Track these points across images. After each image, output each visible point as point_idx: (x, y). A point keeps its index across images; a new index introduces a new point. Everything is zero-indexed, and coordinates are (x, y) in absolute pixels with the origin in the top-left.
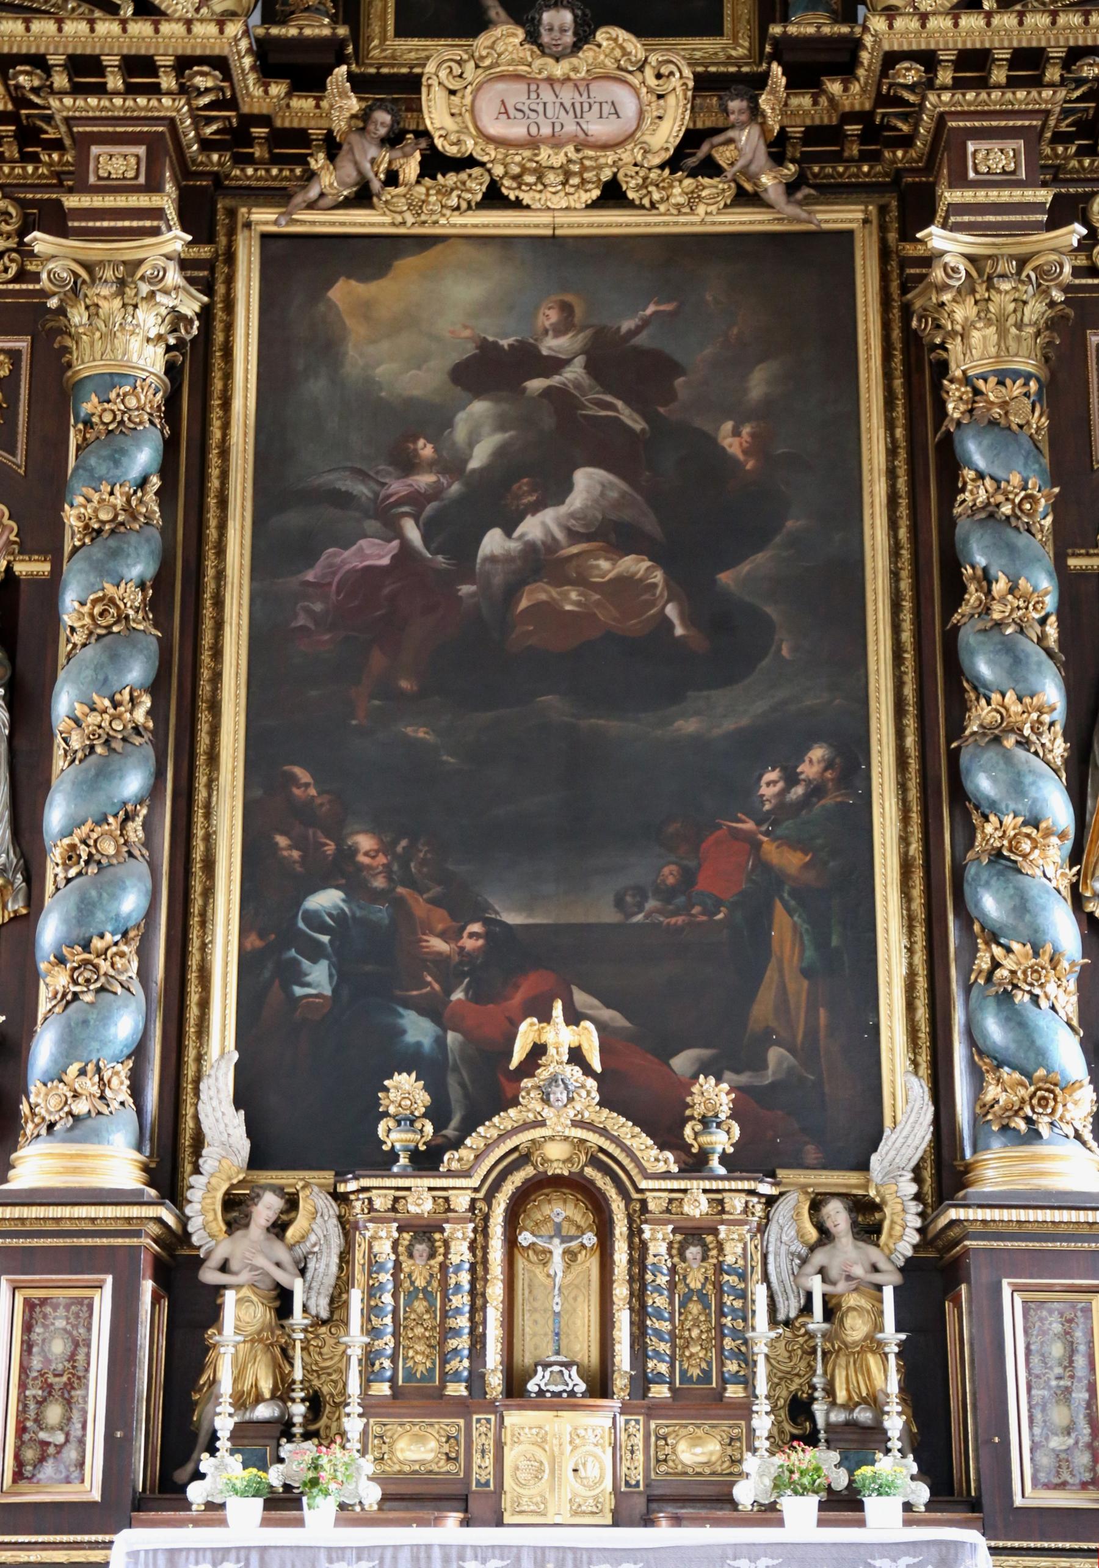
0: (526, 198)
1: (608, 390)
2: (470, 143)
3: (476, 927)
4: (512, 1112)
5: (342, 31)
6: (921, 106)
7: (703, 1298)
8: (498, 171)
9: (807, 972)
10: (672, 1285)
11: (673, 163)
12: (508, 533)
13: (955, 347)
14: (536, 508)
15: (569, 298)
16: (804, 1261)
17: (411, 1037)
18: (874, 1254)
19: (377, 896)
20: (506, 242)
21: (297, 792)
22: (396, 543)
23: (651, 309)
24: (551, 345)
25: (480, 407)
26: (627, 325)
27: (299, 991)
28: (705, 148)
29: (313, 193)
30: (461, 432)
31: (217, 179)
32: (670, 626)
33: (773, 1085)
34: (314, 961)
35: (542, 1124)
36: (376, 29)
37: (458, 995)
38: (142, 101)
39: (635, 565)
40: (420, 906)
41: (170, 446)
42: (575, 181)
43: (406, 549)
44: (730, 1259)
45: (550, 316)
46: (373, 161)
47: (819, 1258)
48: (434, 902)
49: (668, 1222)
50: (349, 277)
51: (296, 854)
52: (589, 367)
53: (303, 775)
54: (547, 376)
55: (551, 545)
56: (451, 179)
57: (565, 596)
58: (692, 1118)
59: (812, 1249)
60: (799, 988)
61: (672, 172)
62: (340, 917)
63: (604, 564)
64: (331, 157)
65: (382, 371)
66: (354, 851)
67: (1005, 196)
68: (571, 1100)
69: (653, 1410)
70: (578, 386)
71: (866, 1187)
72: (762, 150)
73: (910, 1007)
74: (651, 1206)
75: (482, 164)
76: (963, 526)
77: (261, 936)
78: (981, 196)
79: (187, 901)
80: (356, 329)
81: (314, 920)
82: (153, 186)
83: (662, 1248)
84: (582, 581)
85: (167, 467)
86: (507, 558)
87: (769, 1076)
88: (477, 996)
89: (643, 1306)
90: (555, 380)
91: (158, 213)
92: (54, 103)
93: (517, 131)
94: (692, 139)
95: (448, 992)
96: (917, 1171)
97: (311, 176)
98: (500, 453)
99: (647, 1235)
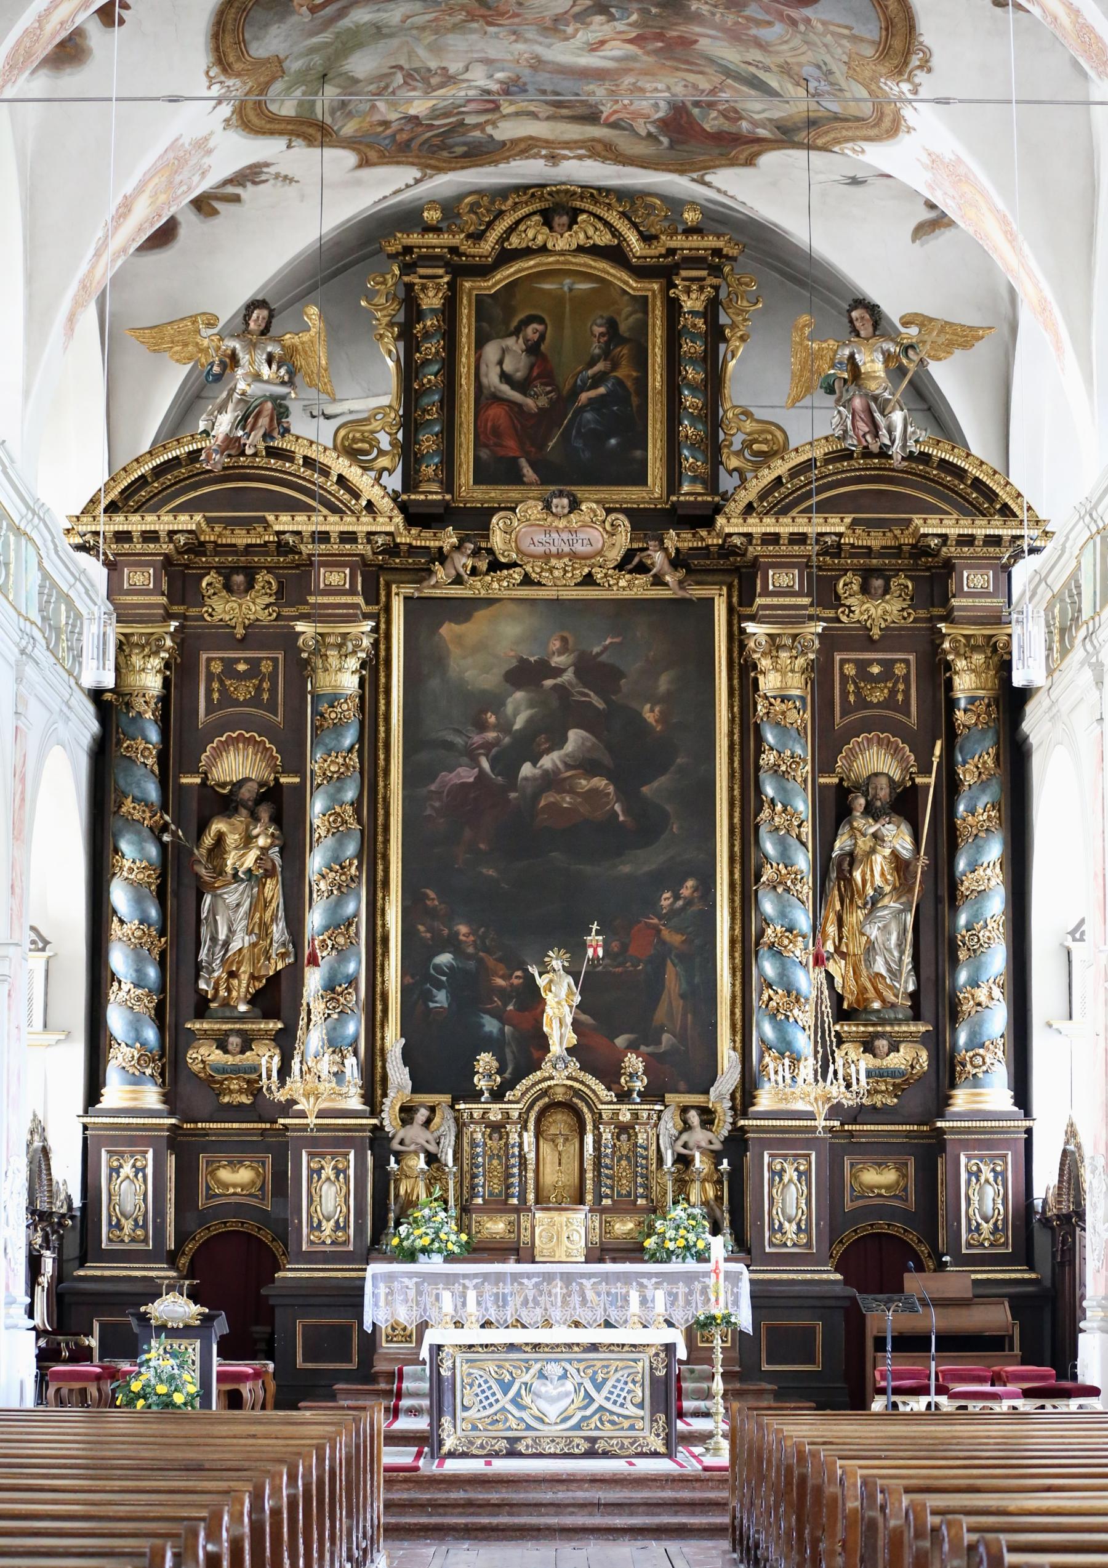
0: (544, 582)
1: (586, 686)
2: (514, 556)
3: (519, 973)
4: (538, 1073)
5: (448, 497)
6: (746, 549)
7: (628, 1158)
8: (529, 569)
9: (682, 996)
10: (613, 1153)
11: (620, 567)
12: (534, 764)
13: (761, 678)
14: (548, 751)
15: (566, 634)
16: (677, 1139)
17: (487, 1028)
18: (710, 1135)
19: (469, 957)
20: (533, 601)
21: (429, 903)
22: (476, 770)
23: (608, 641)
24: (557, 661)
25: (519, 695)
26: (596, 650)
27: (432, 1005)
28: (636, 560)
29: (433, 582)
30: (509, 709)
31: (380, 567)
32: (618, 816)
33: (664, 1053)
34: (439, 989)
35: (552, 1078)
36: (463, 480)
37: (510, 1007)
38: (348, 546)
39: (599, 782)
40: (490, 961)
41: (362, 723)
42: (569, 575)
44: (640, 1141)
45: (556, 644)
46: (464, 566)
47: (685, 1137)
48: (499, 960)
49: (612, 1124)
50: (450, 621)
51: (428, 935)
52: (576, 673)
53: (431, 894)
54: (554, 678)
55: (556, 771)
56: (505, 572)
57: (563, 799)
58: (624, 1074)
59: (681, 1133)
60: (678, 1004)
61: (620, 571)
62: (451, 967)
63: (584, 782)
64: (442, 564)
65: (469, 675)
66: (457, 933)
67: (787, 601)
68: (566, 1067)
69: (604, 1210)
70: (570, 683)
71: (708, 1102)
72: (666, 562)
73: (732, 1013)
74: (604, 1116)
75: (521, 566)
76: (762, 775)
77: (413, 977)
78: (775, 601)
79: (375, 959)
80: (455, 651)
81: (437, 968)
83: (609, 1136)
84: (572, 791)
85: (360, 739)
86: (534, 779)
87: (663, 1048)
88: (521, 1008)
89: (600, 1163)
90: (559, 680)
91: (356, 606)
92: (302, 547)
93: (540, 549)
94: (629, 554)
95: (506, 1005)
96: (733, 1097)
97: (431, 572)
98: (530, 721)
99: (602, 1130)
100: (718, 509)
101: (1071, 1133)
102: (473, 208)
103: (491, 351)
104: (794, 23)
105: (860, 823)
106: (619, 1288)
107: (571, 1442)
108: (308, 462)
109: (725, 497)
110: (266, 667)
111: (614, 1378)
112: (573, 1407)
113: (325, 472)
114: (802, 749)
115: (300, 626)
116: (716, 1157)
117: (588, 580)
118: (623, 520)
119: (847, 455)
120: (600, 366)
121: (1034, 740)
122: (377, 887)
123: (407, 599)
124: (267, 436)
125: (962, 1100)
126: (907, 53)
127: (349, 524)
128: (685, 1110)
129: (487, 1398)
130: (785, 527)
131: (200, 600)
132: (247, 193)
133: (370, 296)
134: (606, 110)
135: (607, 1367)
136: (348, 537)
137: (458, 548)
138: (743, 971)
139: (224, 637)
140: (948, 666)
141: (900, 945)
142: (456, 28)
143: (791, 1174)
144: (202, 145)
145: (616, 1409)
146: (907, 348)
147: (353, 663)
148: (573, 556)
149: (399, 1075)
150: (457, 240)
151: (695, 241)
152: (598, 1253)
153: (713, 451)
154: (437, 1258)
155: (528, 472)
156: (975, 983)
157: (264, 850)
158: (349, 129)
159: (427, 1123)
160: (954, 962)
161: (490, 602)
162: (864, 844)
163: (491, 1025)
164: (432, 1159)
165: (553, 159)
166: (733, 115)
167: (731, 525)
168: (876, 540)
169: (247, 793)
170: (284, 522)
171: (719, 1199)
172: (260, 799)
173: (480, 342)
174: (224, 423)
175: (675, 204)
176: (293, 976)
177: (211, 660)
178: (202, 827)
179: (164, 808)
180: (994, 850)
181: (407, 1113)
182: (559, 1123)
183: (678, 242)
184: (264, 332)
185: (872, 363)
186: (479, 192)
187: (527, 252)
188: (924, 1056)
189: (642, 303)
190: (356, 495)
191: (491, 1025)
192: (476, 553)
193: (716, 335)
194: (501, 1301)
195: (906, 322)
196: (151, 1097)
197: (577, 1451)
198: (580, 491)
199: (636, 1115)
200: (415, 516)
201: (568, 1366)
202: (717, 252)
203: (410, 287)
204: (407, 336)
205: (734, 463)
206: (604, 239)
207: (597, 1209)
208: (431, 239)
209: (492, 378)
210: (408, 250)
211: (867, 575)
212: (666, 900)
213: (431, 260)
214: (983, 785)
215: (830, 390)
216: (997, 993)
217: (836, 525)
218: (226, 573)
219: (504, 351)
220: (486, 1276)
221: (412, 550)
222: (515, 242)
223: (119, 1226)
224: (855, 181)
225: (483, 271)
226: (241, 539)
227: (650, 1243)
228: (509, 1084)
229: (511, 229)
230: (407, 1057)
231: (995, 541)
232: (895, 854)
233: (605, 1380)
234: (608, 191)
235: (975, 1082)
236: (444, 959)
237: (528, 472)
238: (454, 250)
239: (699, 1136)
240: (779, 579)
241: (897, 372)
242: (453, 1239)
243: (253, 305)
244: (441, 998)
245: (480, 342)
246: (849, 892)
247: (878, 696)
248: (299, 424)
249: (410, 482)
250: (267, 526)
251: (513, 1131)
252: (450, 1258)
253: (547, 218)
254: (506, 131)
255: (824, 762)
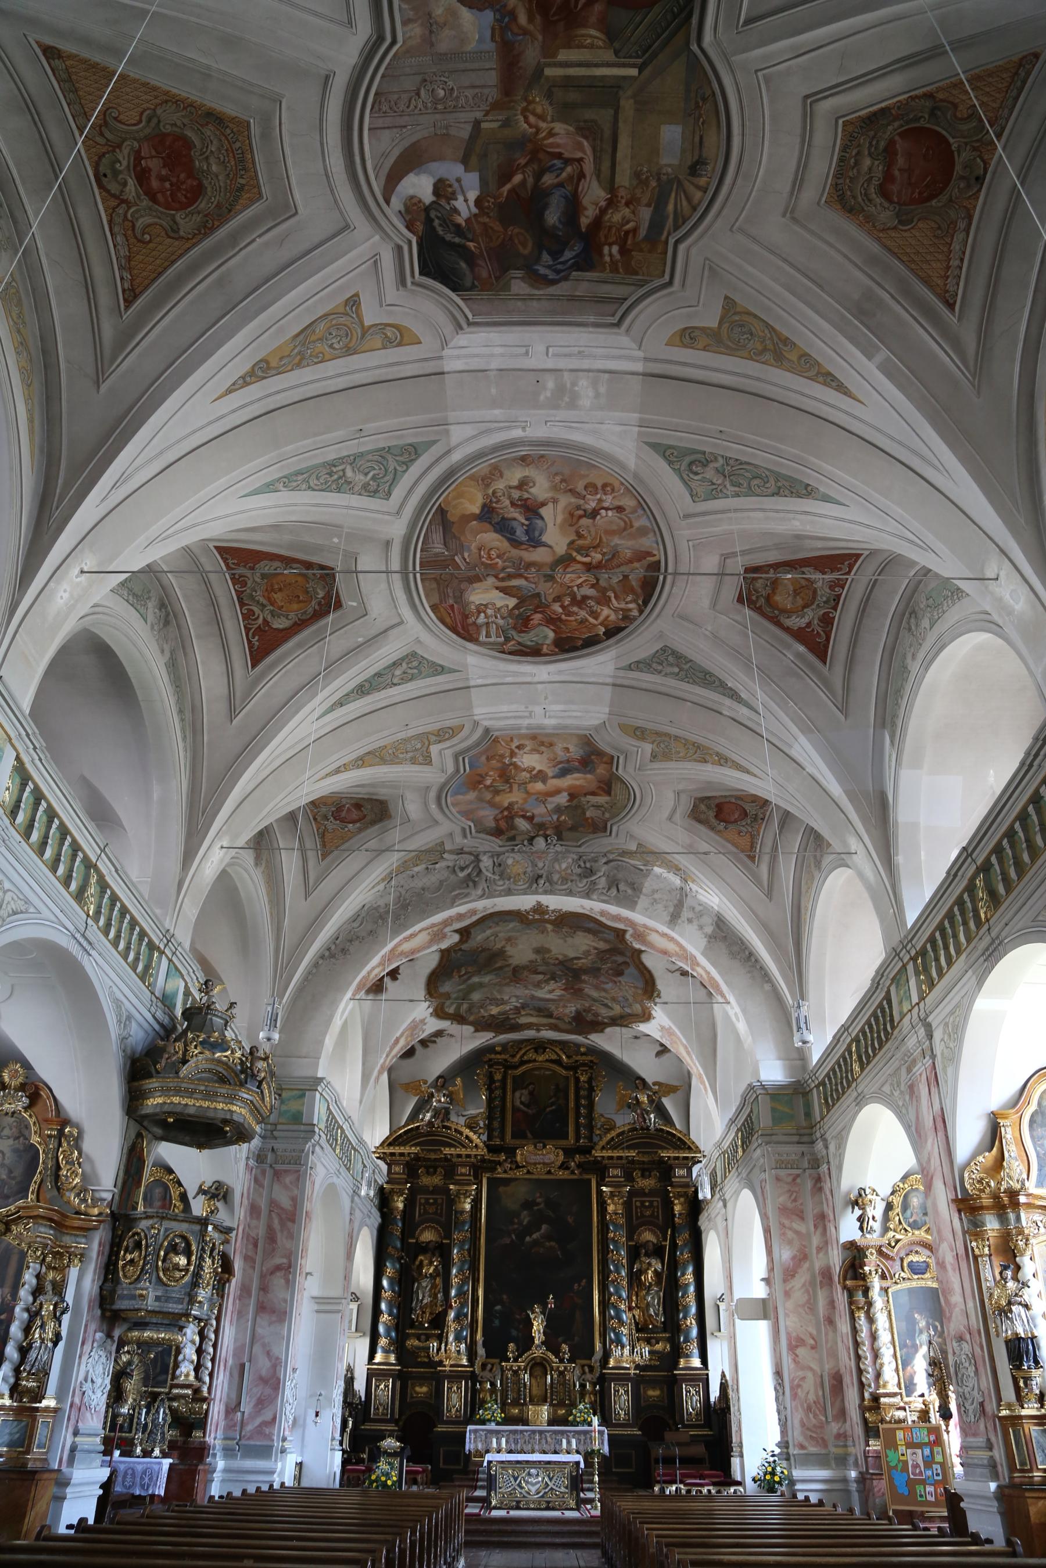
11: (560, 1167)
24: (539, 1200)
39: (553, 1244)
43: (512, 1240)
45: (538, 1195)
82: (469, 1175)
85: (471, 1227)
94: (563, 1163)
97: (496, 1169)
100: (593, 1148)
101: (723, 1375)
102: (512, 1046)
103: (517, 1094)
104: (615, 982)
105: (643, 1259)
106: (559, 1437)
108: (456, 1130)
109: (595, 1144)
110: (439, 1201)
113: (461, 1133)
114: (623, 1232)
115: (451, 1187)
116: (594, 1385)
117: (549, 1172)
118: (561, 1153)
119: (635, 1129)
120: (553, 1100)
121: (702, 1228)
122: (476, 1282)
123: (488, 1178)
124: (442, 1121)
125: (682, 1363)
126: (653, 992)
127: (468, 1152)
128: (583, 1366)
130: (616, 1154)
131: (418, 1177)
132: (438, 1040)
133: (478, 1075)
134: (555, 1013)
136: (468, 1156)
137: (505, 1161)
138: (603, 1313)
139: (425, 1190)
140: (672, 1203)
141: (658, 1303)
142: (507, 984)
143: (621, 1391)
144: (423, 1022)
146: (655, 1093)
147: (469, 1200)
148: (544, 1164)
149: (481, 1351)
150: (506, 1057)
151: (584, 1058)
152: (551, 1423)
153: (590, 1128)
154: (493, 1424)
155: (529, 1135)
156: (685, 1318)
157: (436, 1266)
158: (471, 1018)
159: (491, 1370)
160: (678, 1311)
161: (516, 1179)
162: (644, 1266)
163: (514, 1333)
164: (493, 1384)
165: (538, 1030)
166: (596, 1015)
167: (597, 1153)
168: (646, 1159)
169: (431, 1246)
170: (447, 1151)
171: (596, 1401)
172: (436, 1248)
173: (514, 1092)
174: (428, 1116)
175: (578, 1046)
176: (445, 1313)
177: (421, 1198)
178: (416, 1258)
179: (402, 1250)
180: (690, 1269)
181: (484, 1366)
182: (538, 1371)
183: (579, 1058)
184: (443, 1086)
185: (644, 1099)
186: (514, 1041)
187: (529, 1062)
188: (668, 1347)
189: (567, 1078)
190: (471, 1141)
191: (514, 1333)
192: (511, 1163)
193: (591, 1090)
194: (516, 1442)
195: (655, 1084)
196: (392, 1359)
198: (546, 1142)
199: (565, 1368)
200: (491, 1149)
202: (591, 1061)
203: (491, 1072)
204: (490, 1090)
205: (598, 1132)
206: (554, 1057)
207: (551, 1405)
208: (498, 1056)
209: (518, 1103)
210: (490, 1060)
211: (643, 1171)
212: (576, 1286)
213: (498, 1063)
214: (685, 1245)
215: (629, 1107)
216: (694, 1322)
217: (633, 1153)
218: (427, 1168)
219: (522, 1094)
220: (511, 1431)
221: (490, 1161)
222: (525, 1058)
223: (378, 1409)
224: (636, 1037)
225: (515, 1067)
226: (433, 1156)
227: (571, 1418)
228: (520, 1356)
229: (524, 1054)
230: (484, 1345)
231: (686, 1158)
232: (656, 1271)
234: (556, 1041)
235: (688, 1356)
236: (498, 1308)
237: (529, 1135)
238: (506, 1060)
239: (588, 1376)
240: (613, 1172)
241: (651, 1101)
242: (499, 1416)
243: (439, 1077)
244: (497, 1322)
245: (514, 1092)
246: (640, 1284)
247: (648, 1213)
248: (453, 1118)
249: (490, 1138)
250: (441, 1152)
251: (521, 1373)
252: (498, 1424)
253: (536, 1050)
254: (523, 1020)
255: (630, 1238)
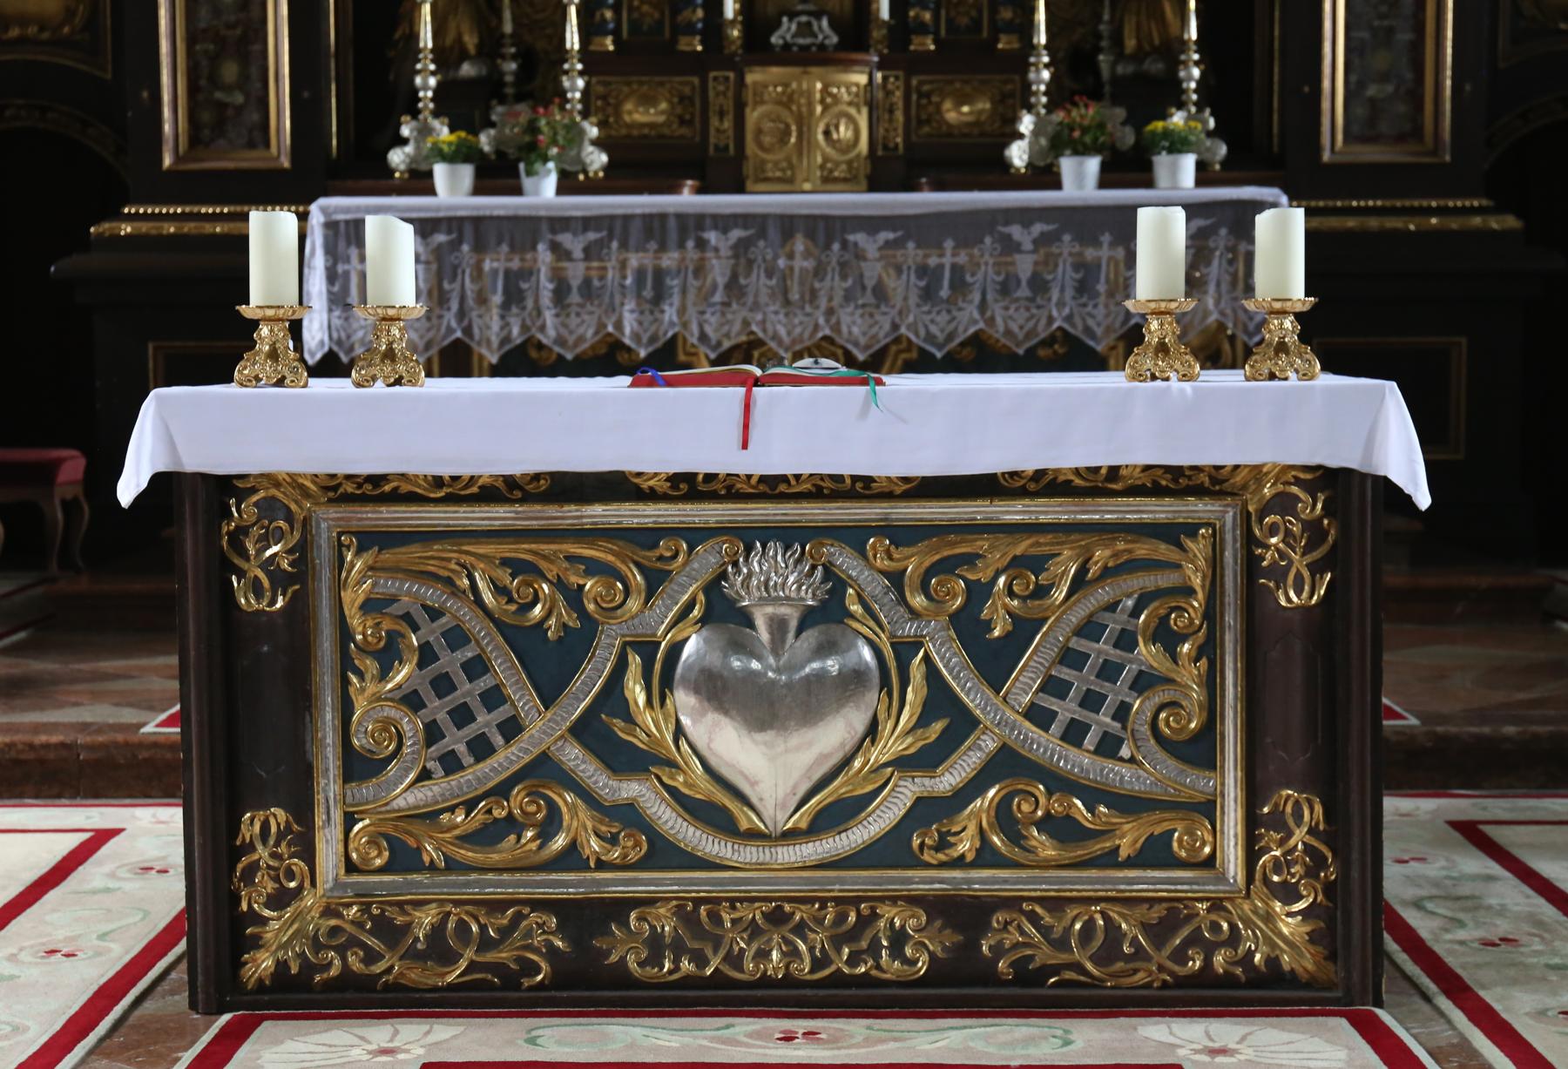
107: (866, 921)
111: (1076, 617)
112: (880, 753)
129: (462, 716)
135: (1036, 563)
145: (1080, 762)
197: (892, 968)
201: (845, 560)
233: (1023, 629)
